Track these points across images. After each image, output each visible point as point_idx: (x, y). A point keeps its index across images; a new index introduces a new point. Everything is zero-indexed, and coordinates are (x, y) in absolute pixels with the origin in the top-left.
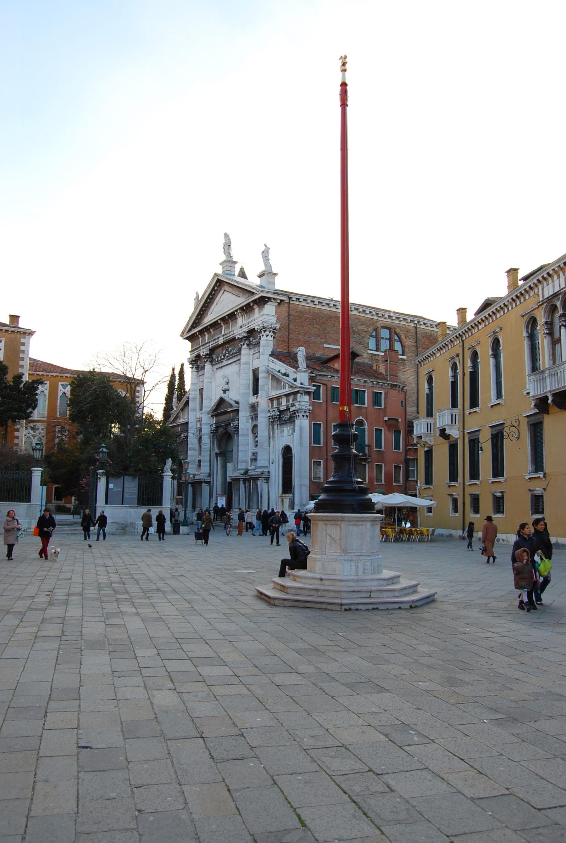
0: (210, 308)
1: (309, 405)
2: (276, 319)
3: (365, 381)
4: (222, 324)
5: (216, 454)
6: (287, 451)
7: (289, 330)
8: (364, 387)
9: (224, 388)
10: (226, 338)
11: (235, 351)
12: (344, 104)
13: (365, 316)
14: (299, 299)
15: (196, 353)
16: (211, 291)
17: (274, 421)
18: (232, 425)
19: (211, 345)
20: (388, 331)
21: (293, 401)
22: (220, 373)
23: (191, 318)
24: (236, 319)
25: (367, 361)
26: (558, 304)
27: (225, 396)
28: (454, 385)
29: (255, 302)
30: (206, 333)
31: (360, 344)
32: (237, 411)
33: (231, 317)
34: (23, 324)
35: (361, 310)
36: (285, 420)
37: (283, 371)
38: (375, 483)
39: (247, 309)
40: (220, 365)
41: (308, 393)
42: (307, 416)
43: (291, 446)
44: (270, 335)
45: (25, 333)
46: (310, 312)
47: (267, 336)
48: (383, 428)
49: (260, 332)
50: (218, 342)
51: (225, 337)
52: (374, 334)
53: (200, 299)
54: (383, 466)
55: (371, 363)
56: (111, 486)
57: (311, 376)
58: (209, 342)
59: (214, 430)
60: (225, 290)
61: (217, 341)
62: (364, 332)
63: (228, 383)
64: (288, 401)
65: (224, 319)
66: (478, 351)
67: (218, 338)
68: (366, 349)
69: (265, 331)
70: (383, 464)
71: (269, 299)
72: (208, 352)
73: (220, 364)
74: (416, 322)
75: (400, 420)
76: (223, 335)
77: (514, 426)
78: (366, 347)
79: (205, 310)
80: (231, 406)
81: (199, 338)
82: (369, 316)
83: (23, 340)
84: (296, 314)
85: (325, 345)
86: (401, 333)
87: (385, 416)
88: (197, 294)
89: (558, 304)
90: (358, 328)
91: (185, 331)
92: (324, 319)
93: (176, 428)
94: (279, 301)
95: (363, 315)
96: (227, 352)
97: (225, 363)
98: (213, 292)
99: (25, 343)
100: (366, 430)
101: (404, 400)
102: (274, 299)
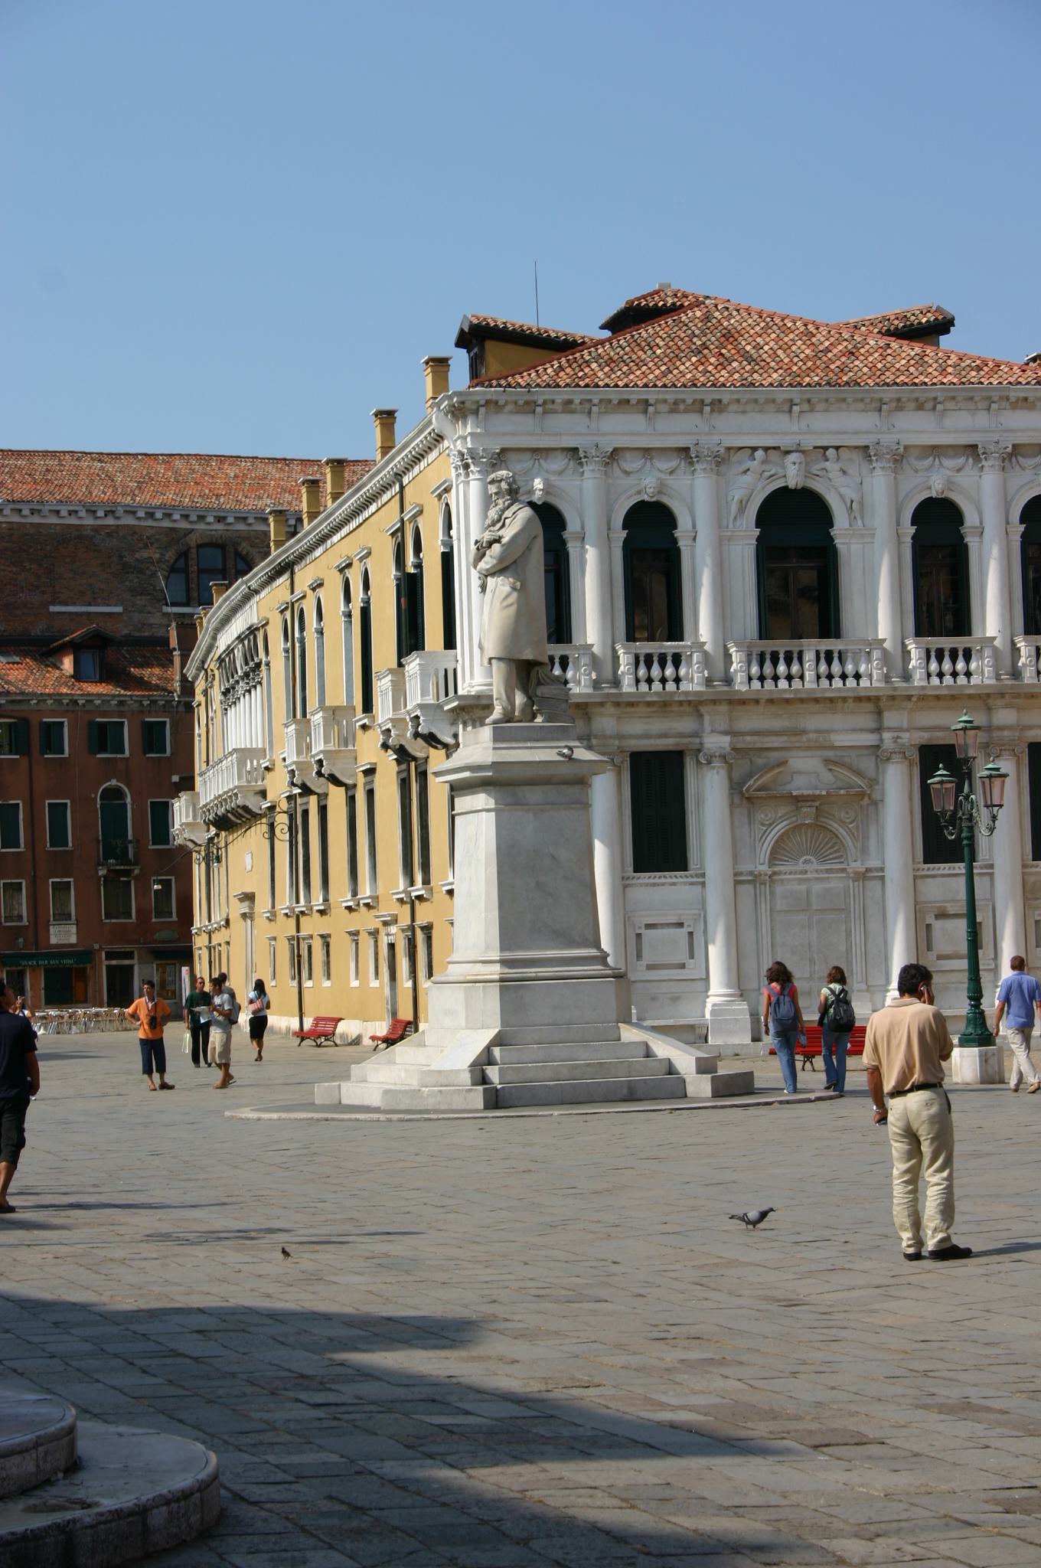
8: (121, 714)
13: (155, 524)
20: (219, 552)
31: (141, 594)
46: (12, 535)
52: (181, 564)
54: (173, 881)
68: (157, 605)
78: (159, 601)
82: (166, 524)
85: (53, 609)
90: (137, 555)
92: (48, 548)
95: (150, 523)
100: (129, 807)
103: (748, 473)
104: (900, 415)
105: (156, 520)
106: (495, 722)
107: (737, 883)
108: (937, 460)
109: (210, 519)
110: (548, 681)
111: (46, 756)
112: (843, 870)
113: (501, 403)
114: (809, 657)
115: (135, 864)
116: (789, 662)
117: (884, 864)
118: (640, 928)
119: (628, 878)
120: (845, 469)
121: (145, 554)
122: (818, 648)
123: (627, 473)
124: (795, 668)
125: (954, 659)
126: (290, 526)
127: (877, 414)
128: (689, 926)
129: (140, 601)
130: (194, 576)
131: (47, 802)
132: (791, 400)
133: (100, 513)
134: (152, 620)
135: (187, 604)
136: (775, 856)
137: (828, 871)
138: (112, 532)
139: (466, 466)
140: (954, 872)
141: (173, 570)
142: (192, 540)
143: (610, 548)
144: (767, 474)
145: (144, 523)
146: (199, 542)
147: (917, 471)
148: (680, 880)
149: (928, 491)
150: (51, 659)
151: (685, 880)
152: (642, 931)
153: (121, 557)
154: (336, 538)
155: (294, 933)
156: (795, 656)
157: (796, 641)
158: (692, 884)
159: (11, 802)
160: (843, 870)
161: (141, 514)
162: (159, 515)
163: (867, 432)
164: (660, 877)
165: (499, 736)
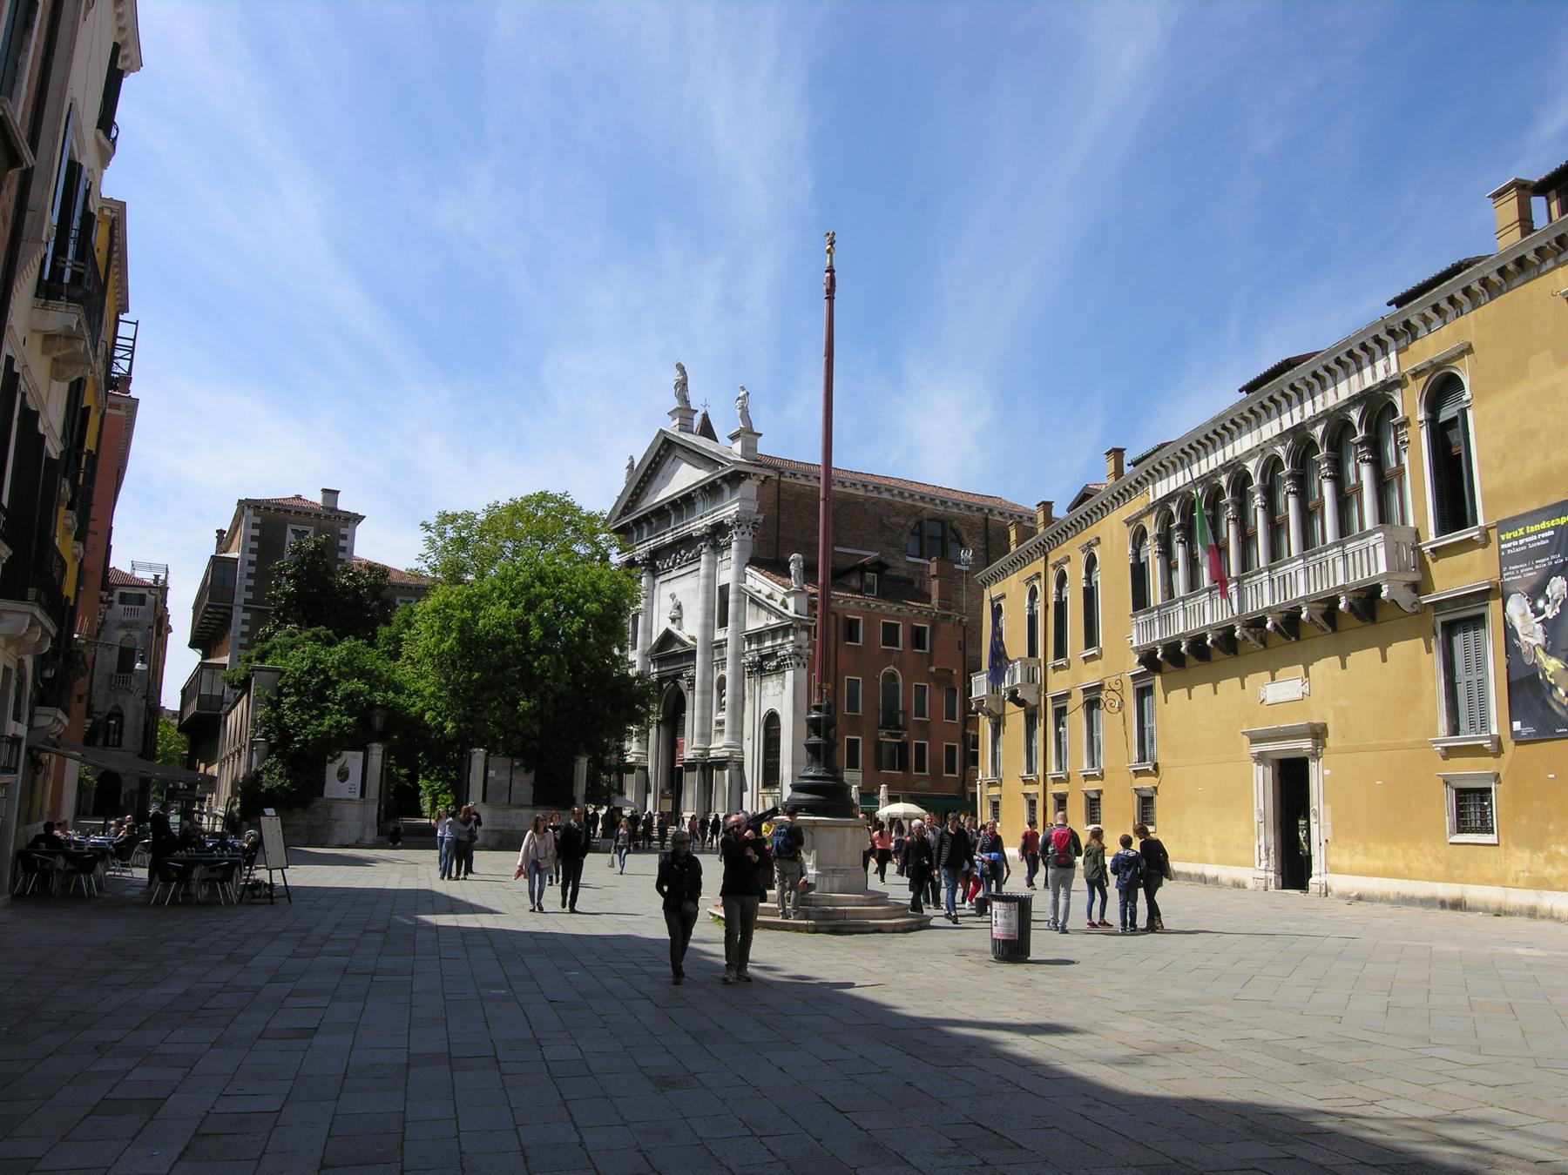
0: (651, 484)
1: (809, 648)
2: (757, 506)
3: (899, 610)
4: (671, 512)
6: (772, 720)
7: (779, 524)
8: (898, 618)
9: (673, 614)
11: (691, 555)
12: (830, 297)
13: (903, 501)
14: (795, 475)
16: (655, 457)
17: (751, 671)
18: (684, 675)
19: (653, 543)
23: (620, 498)
24: (695, 504)
25: (904, 574)
26: (1174, 508)
27: (673, 628)
28: (1032, 620)
29: (724, 478)
30: (644, 525)
32: (692, 654)
33: (684, 503)
34: (343, 505)
36: (769, 671)
38: (914, 773)
39: (711, 491)
40: (667, 577)
41: (808, 629)
42: (804, 665)
43: (779, 712)
45: (347, 519)
47: (743, 534)
48: (927, 685)
49: (731, 528)
53: (635, 467)
55: (911, 577)
56: (492, 773)
57: (811, 601)
58: (650, 539)
60: (676, 456)
61: (662, 537)
62: (901, 527)
66: (1066, 571)
69: (739, 526)
70: (927, 743)
71: (747, 475)
73: (667, 574)
74: (986, 511)
75: (955, 672)
76: (673, 530)
77: (1113, 690)
78: (904, 552)
79: (644, 487)
81: (633, 532)
82: (909, 501)
83: (343, 531)
84: (791, 499)
85: (836, 549)
86: (962, 528)
87: (931, 665)
88: (631, 458)
89: (1174, 508)
90: (891, 520)
94: (763, 479)
96: (678, 556)
97: (675, 573)
99: (346, 536)
101: (961, 639)
102: (754, 474)
109: (938, 502)
111: (847, 643)
115: (905, 729)
121: (896, 520)
126: (984, 514)
129: (892, 550)
130: (926, 539)
131: (846, 677)
133: (871, 488)
134: (898, 565)
135: (920, 557)
138: (877, 502)
141: (912, 533)
142: (925, 514)
146: (930, 517)
150: (840, 580)
153: (881, 520)
161: (896, 492)
162: (907, 495)
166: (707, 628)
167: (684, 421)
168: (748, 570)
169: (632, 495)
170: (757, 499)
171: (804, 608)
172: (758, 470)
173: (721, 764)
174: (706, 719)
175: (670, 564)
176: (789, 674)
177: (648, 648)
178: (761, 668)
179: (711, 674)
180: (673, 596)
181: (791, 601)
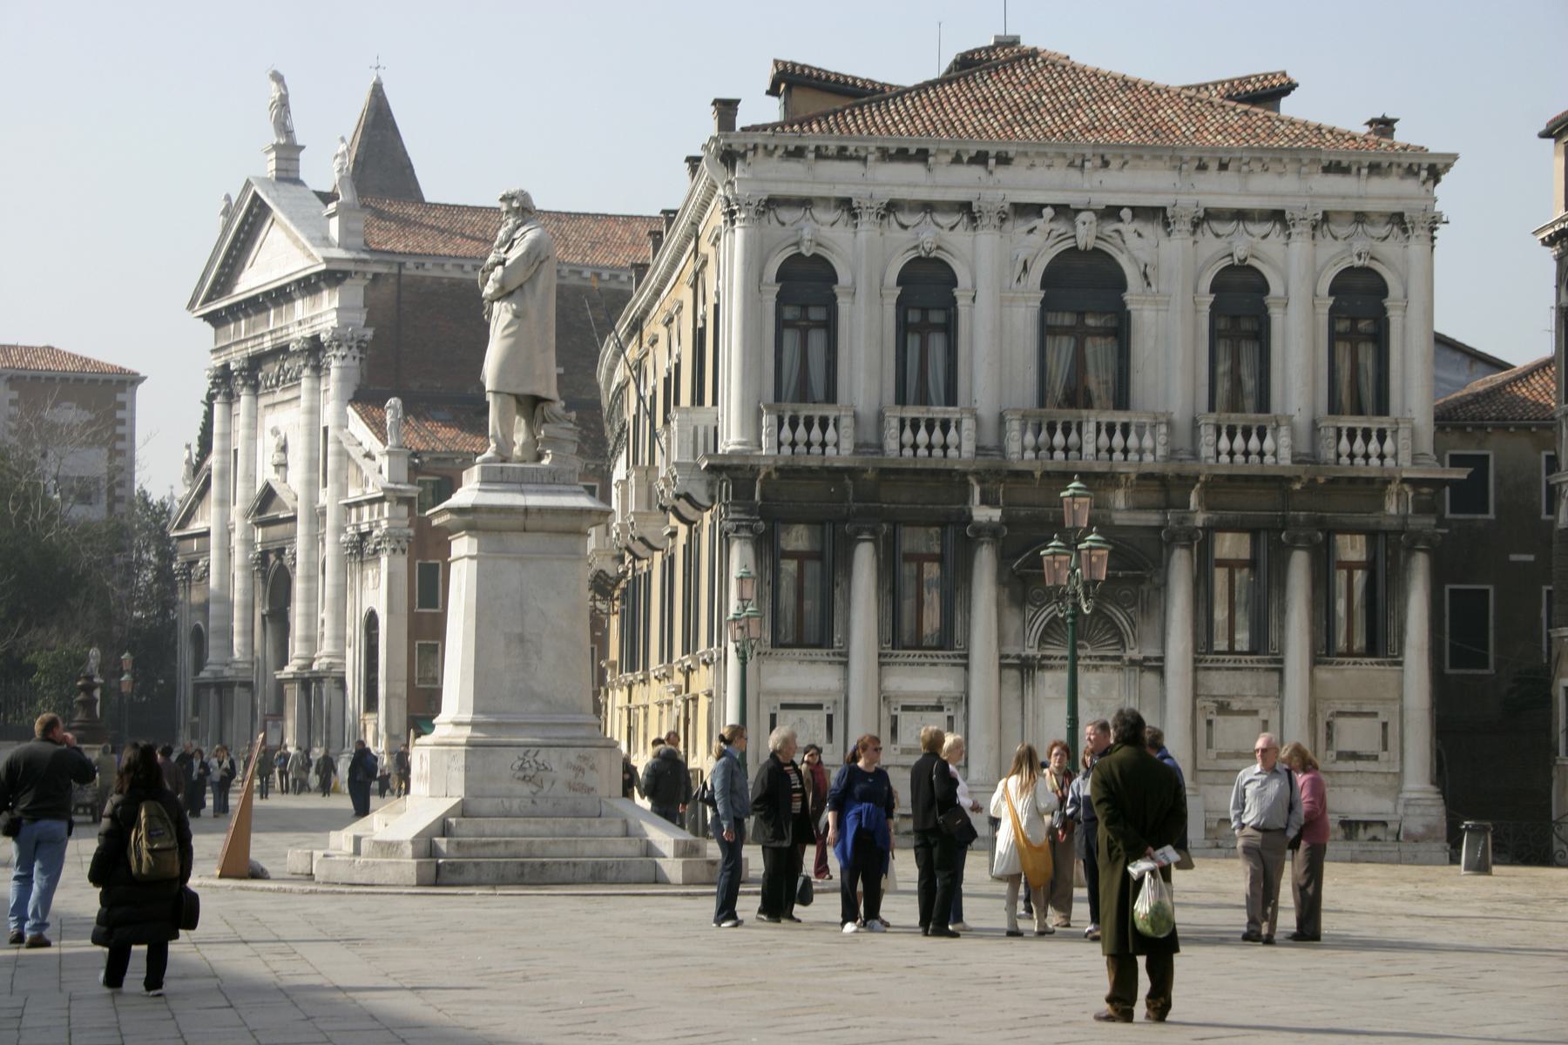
1: (409, 526)
2: (364, 316)
5: (263, 616)
6: (371, 620)
10: (277, 339)
15: (223, 359)
19: (251, 348)
21: (379, 515)
22: (270, 419)
32: (293, 519)
33: (280, 296)
35: (587, 274)
37: (367, 447)
42: (403, 551)
44: (350, 355)
50: (262, 343)
51: (274, 336)
58: (246, 340)
59: (258, 559)
61: (260, 340)
63: (284, 449)
64: (371, 514)
65: (267, 294)
67: (262, 335)
71: (346, 274)
72: (246, 365)
76: (271, 332)
80: (284, 507)
88: (228, 198)
91: (197, 298)
93: (187, 542)
94: (370, 276)
97: (280, 396)
98: (251, 219)
102: (356, 273)
103: (1035, 231)
104: (1201, 176)
105: (603, 281)
106: (486, 461)
107: (1002, 667)
108: (1241, 225)
110: (554, 418)
112: (1118, 658)
113: (771, 147)
114: (1089, 429)
116: (1066, 433)
117: (1164, 652)
118: (896, 709)
119: (885, 656)
120: (1140, 231)
122: (1099, 420)
123: (904, 227)
124: (1073, 437)
125: (1247, 436)
127: (1176, 173)
128: (949, 710)
132: (1084, 155)
136: (1043, 641)
137: (1103, 658)
139: (732, 213)
140: (1240, 665)
143: (883, 305)
144: (1054, 233)
145: (588, 284)
147: (1217, 236)
148: (941, 660)
149: (1229, 258)
151: (947, 660)
152: (899, 713)
154: (665, 292)
155: (626, 703)
156: (1074, 427)
157: (1074, 412)
158: (954, 665)
159: (431, 561)
160: (1118, 658)
163: (1165, 192)
164: (920, 656)
165: (490, 479)
166: (312, 486)
167: (284, 165)
168: (350, 410)
169: (223, 266)
170: (365, 306)
171: (403, 474)
172: (360, 267)
173: (319, 678)
174: (310, 617)
175: (274, 382)
176: (384, 560)
177: (250, 504)
178: (359, 549)
179: (315, 553)
180: (275, 432)
181: (384, 462)
